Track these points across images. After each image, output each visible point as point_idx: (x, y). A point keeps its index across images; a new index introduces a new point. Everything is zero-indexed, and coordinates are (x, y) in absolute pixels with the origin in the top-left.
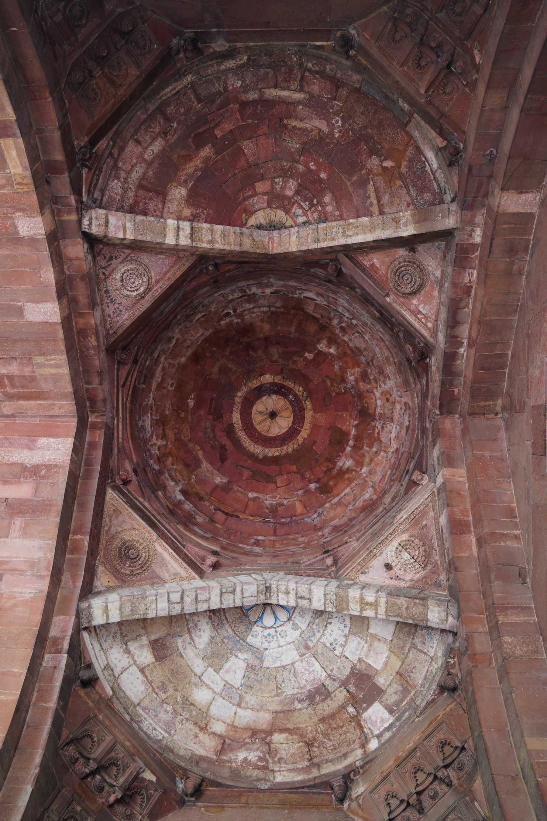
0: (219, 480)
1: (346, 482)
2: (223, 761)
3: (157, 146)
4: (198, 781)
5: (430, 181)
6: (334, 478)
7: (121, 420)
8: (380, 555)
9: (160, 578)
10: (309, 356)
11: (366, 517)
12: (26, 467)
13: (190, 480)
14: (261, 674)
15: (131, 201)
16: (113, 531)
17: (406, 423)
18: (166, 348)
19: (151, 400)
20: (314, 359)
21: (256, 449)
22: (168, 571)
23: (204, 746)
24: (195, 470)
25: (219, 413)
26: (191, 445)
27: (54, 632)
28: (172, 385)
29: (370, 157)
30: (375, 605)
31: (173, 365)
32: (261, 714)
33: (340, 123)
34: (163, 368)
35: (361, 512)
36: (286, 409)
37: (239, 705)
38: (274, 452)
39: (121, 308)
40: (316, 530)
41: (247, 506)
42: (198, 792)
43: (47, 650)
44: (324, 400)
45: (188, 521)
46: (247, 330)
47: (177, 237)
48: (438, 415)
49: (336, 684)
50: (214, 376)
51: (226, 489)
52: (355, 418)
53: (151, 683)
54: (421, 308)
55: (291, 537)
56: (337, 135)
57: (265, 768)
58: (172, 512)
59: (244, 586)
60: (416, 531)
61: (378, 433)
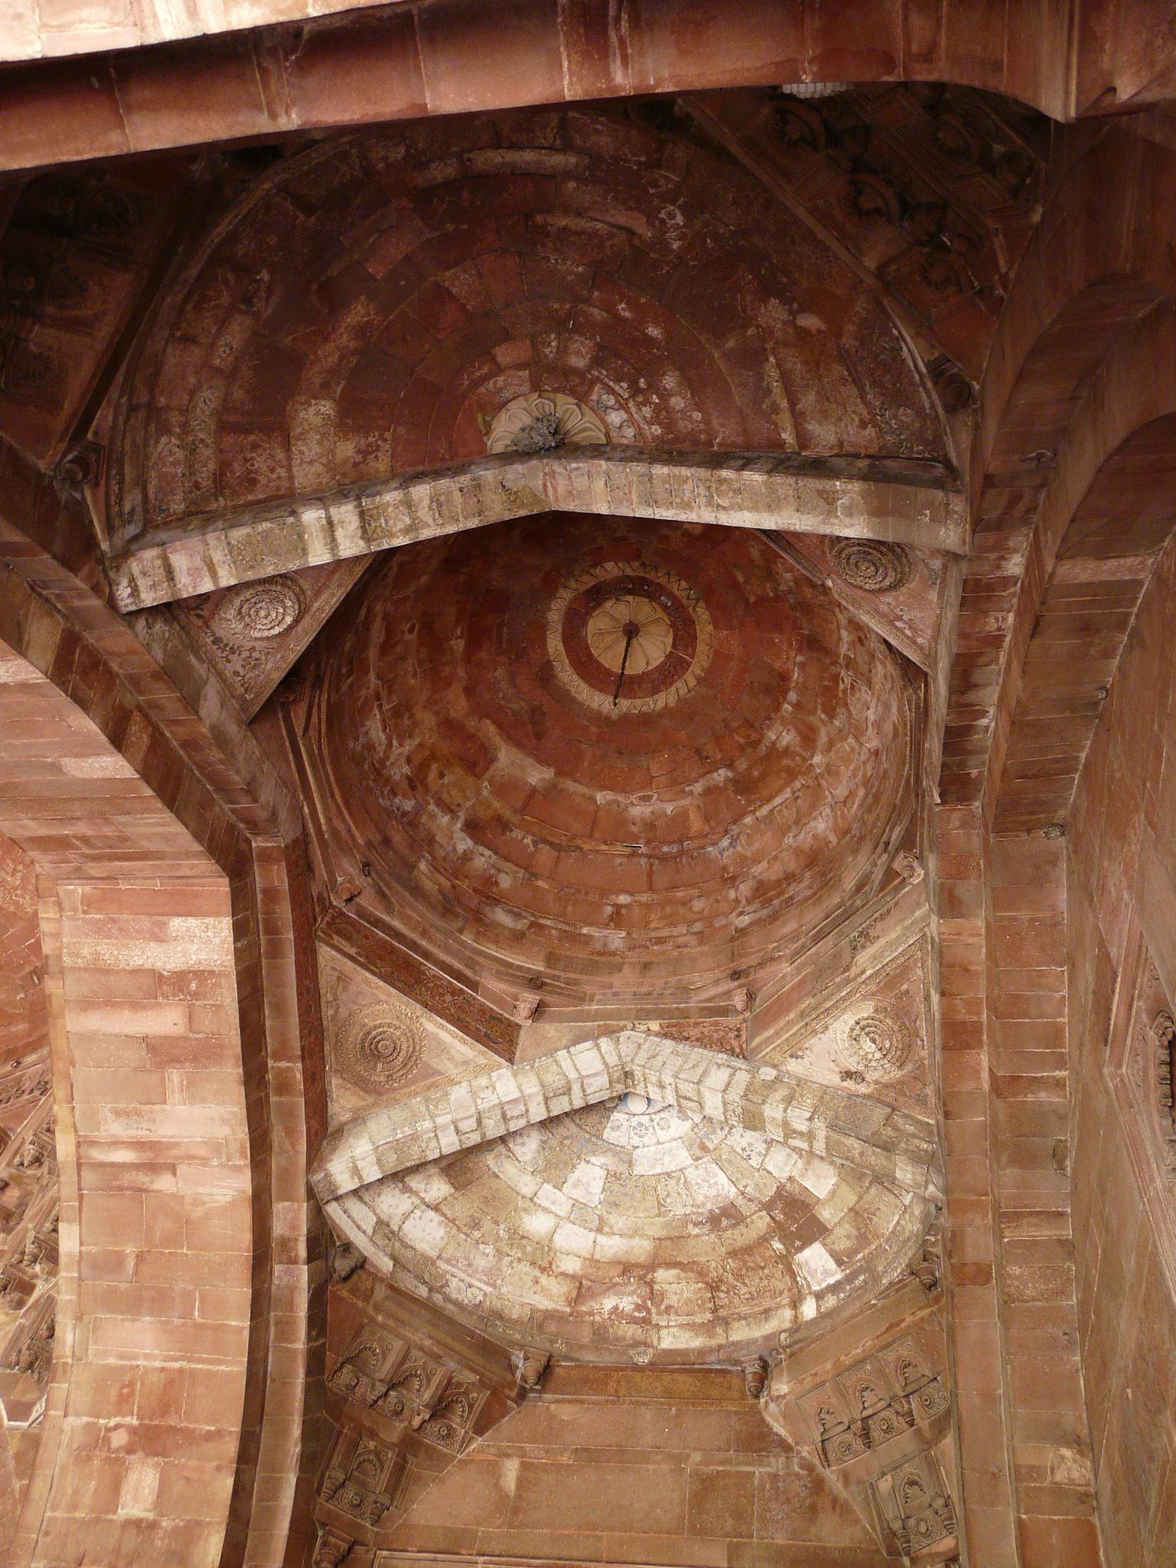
1: (784, 775)
2: (582, 1314)
3: (236, 335)
4: (544, 1360)
5: (912, 384)
9: (440, 1074)
12: (161, 976)
15: (212, 466)
16: (343, 1012)
22: (451, 1059)
23: (550, 1296)
24: (486, 769)
27: (278, 1229)
28: (411, 630)
29: (765, 301)
32: (636, 1242)
33: (680, 219)
37: (599, 1230)
39: (256, 655)
40: (725, 881)
41: (594, 822)
42: (546, 1373)
43: (275, 1258)
47: (333, 543)
51: (553, 791)
53: (453, 1221)
56: (675, 246)
57: (646, 1321)
59: (586, 1064)
61: (845, 691)
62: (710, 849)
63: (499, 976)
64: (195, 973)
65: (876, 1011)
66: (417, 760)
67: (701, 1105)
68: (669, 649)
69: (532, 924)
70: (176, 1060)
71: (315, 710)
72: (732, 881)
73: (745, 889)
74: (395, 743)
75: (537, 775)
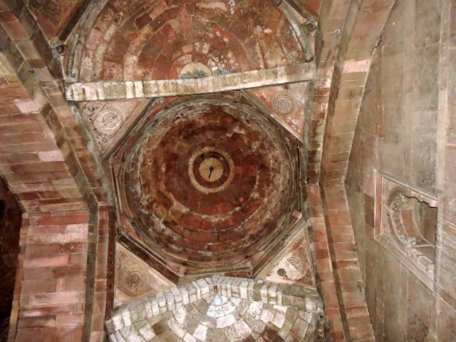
3: (112, 30)
5: (296, 43)
12: (61, 245)
13: (168, 214)
14: (216, 332)
15: (100, 70)
19: (139, 174)
20: (232, 137)
24: (170, 207)
29: (256, 27)
30: (276, 299)
33: (234, 4)
34: (144, 155)
41: (201, 224)
46: (191, 124)
49: (257, 336)
51: (189, 215)
54: (293, 121)
55: (227, 242)
56: (232, 12)
58: (158, 241)
62: (236, 229)
63: (173, 261)
64: (73, 243)
66: (150, 201)
67: (239, 294)
69: (183, 250)
70: (62, 275)
72: (243, 236)
73: (247, 238)
75: (185, 210)
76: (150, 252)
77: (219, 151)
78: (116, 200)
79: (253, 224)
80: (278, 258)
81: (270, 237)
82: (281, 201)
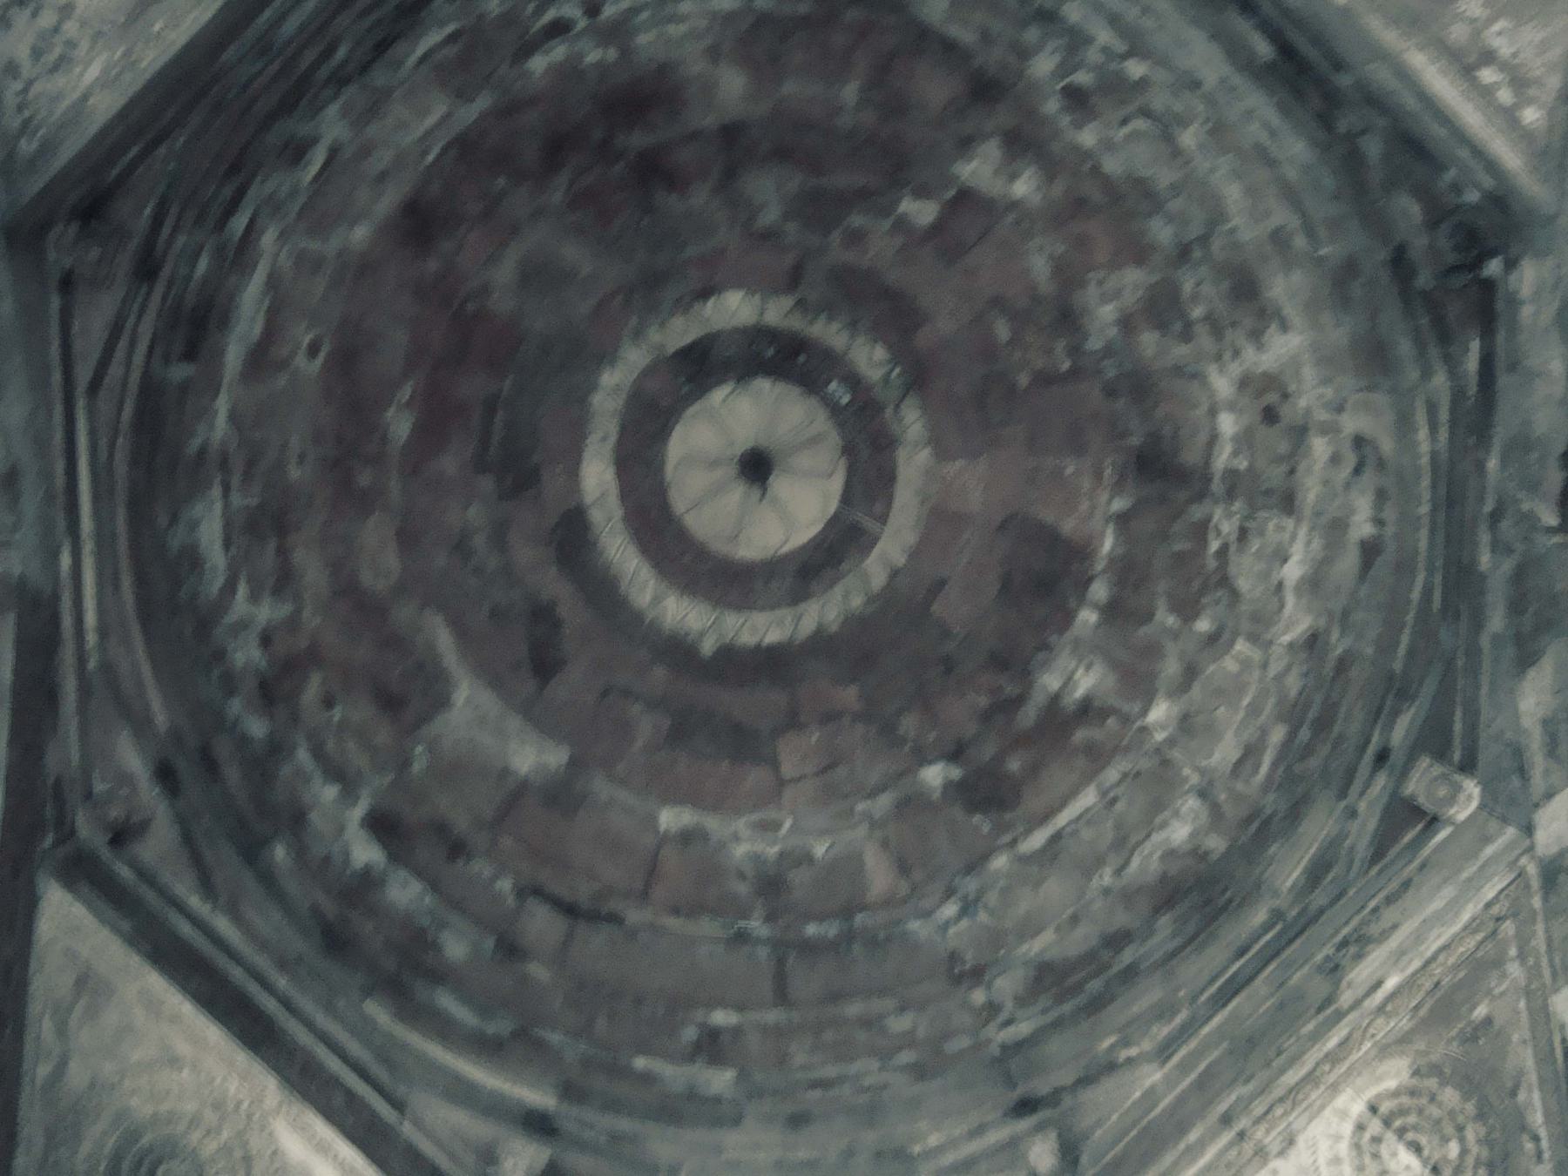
0: (532, 757)
6: (1022, 740)
7: (88, 547)
8: (1282, 1153)
10: (921, 211)
11: (1193, 941)
13: (406, 763)
16: (77, 1076)
17: (1362, 527)
18: (285, 189)
20: (937, 228)
21: (682, 613)
24: (424, 719)
25: (522, 469)
26: (403, 613)
28: (313, 350)
31: (317, 264)
34: (273, 283)
35: (1157, 911)
36: (814, 441)
38: (763, 628)
41: (652, 870)
44: (983, 403)
45: (405, 971)
46: (642, 96)
48: (1551, 531)
50: (502, 303)
51: (561, 796)
52: (1118, 487)
54: (1500, 38)
55: (853, 1009)
58: (335, 941)
60: (1443, 1048)
61: (1223, 552)
62: (914, 925)
65: (1416, 1073)
68: (833, 506)
71: (123, 344)
72: (977, 975)
73: (1006, 985)
74: (242, 590)
76: (287, 1004)
77: (829, 333)
78: (66, 561)
79: (1055, 890)
80: (1292, 1096)
81: (1211, 962)
82: (1293, 714)
